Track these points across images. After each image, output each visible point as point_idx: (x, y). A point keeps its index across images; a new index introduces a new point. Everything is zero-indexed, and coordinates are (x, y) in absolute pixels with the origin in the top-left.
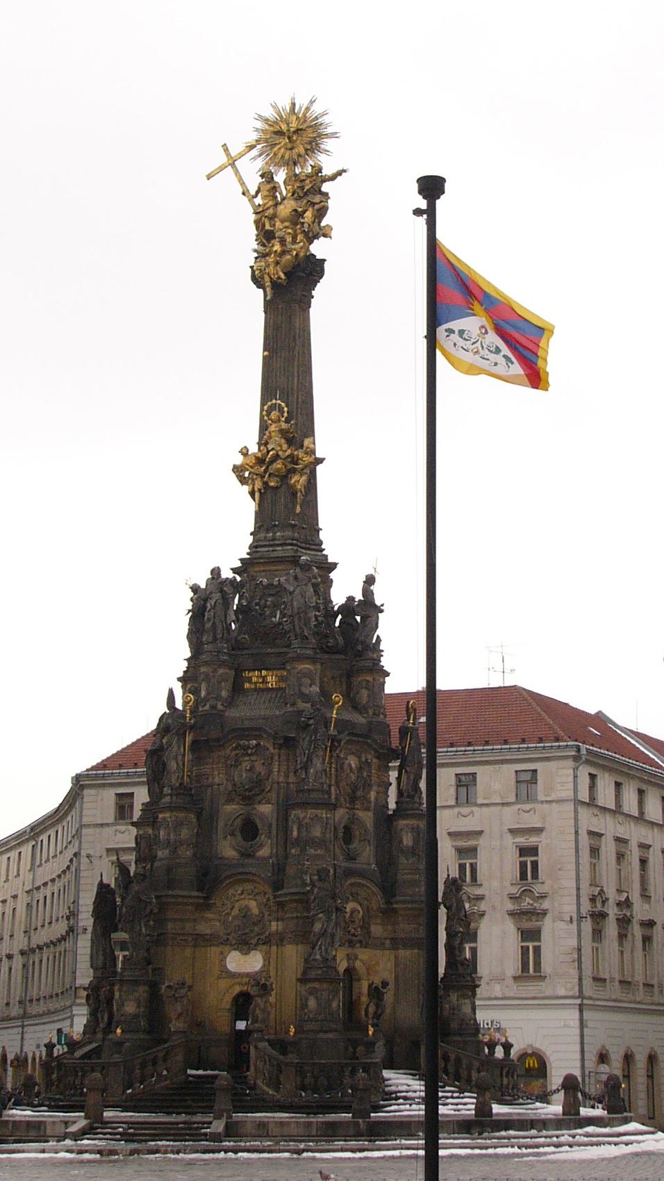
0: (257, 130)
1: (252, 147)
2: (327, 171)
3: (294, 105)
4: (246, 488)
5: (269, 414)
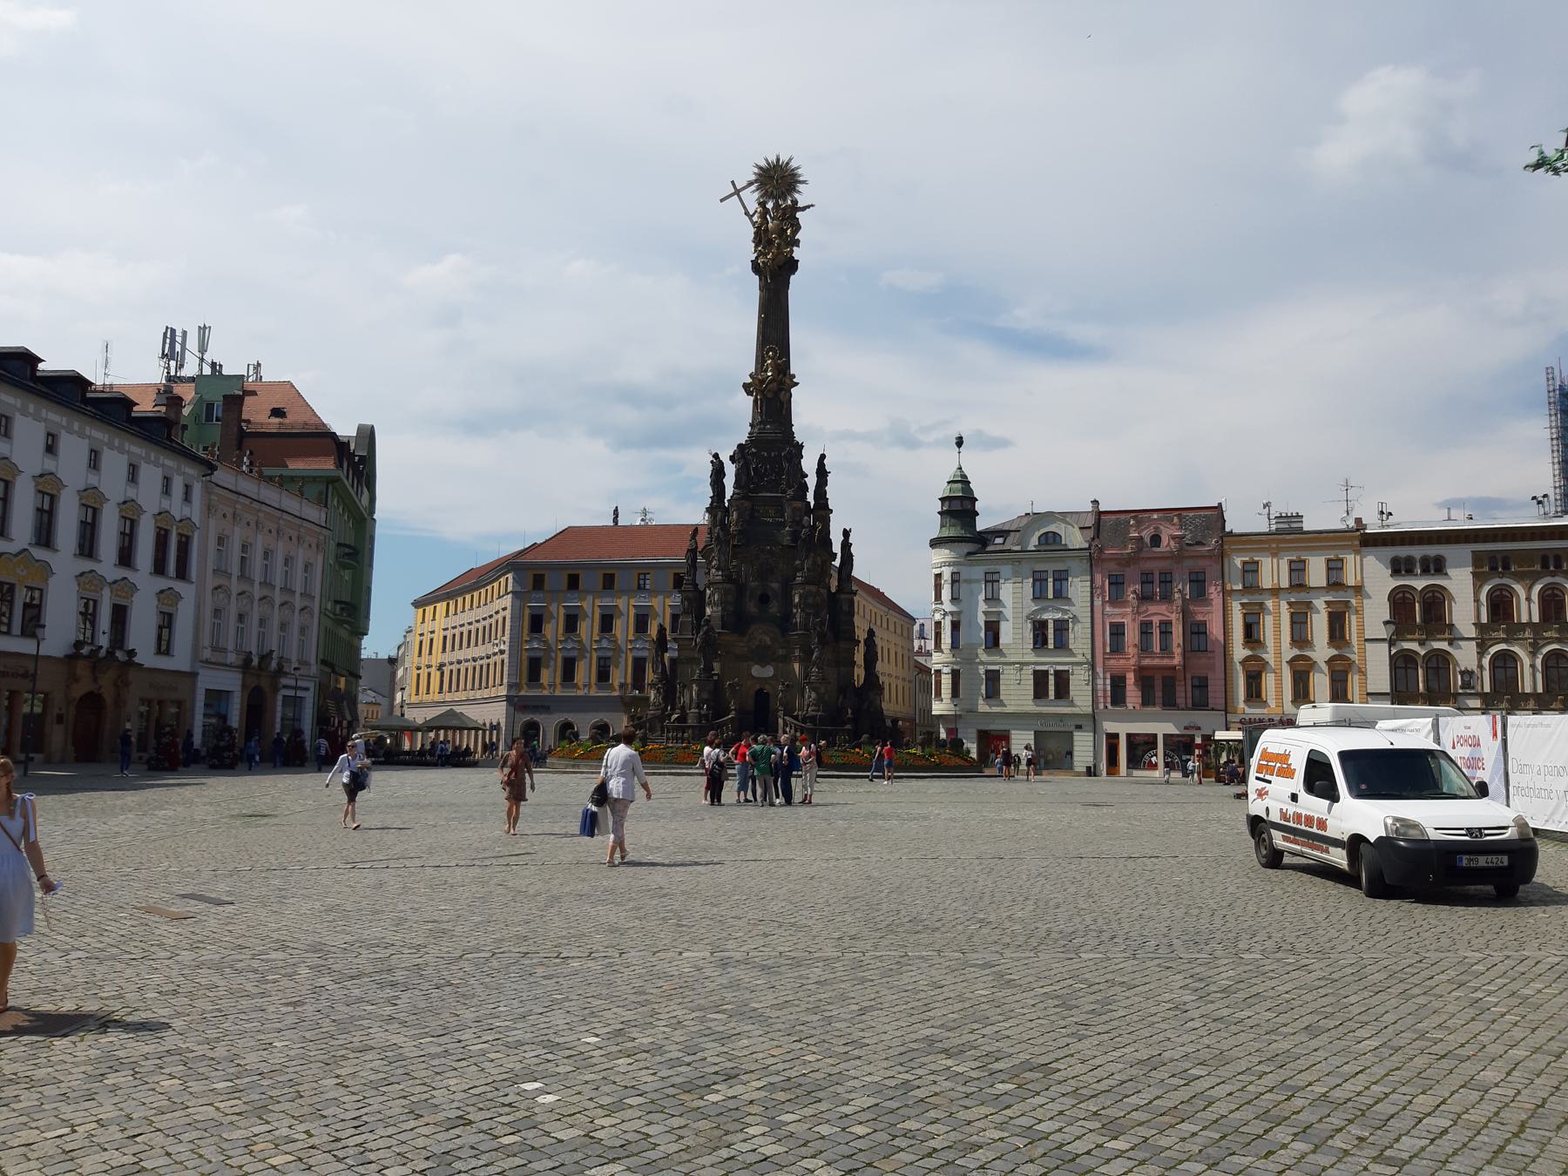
4: (751, 398)
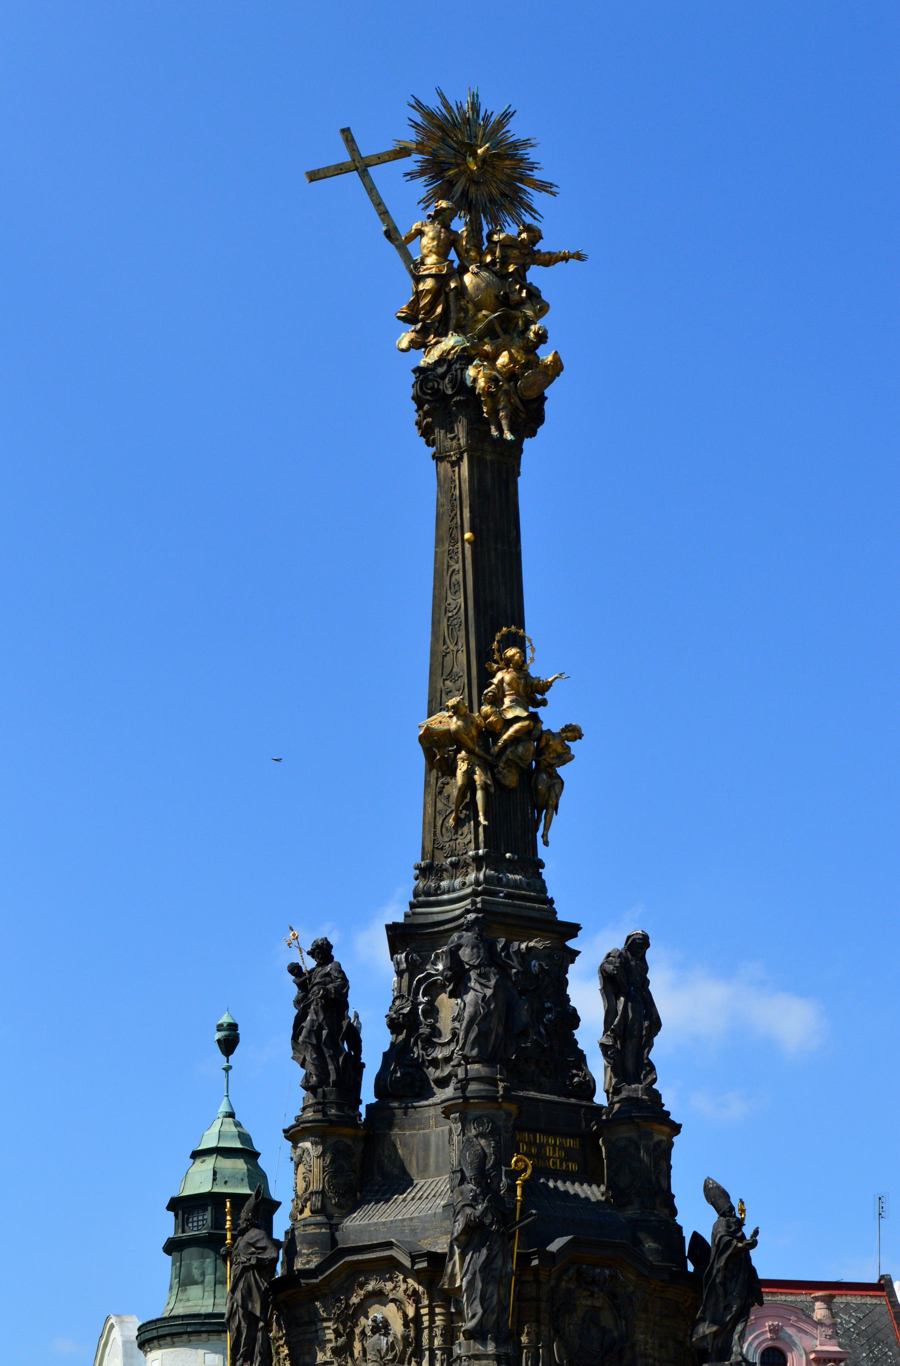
0: (416, 125)
1: (402, 152)
3: (475, 107)
5: (501, 650)
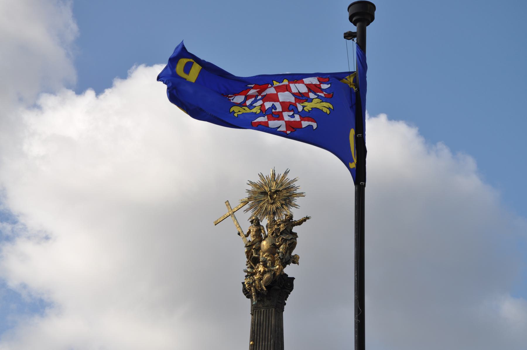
0: (249, 191)
2: (296, 218)
3: (274, 174)
